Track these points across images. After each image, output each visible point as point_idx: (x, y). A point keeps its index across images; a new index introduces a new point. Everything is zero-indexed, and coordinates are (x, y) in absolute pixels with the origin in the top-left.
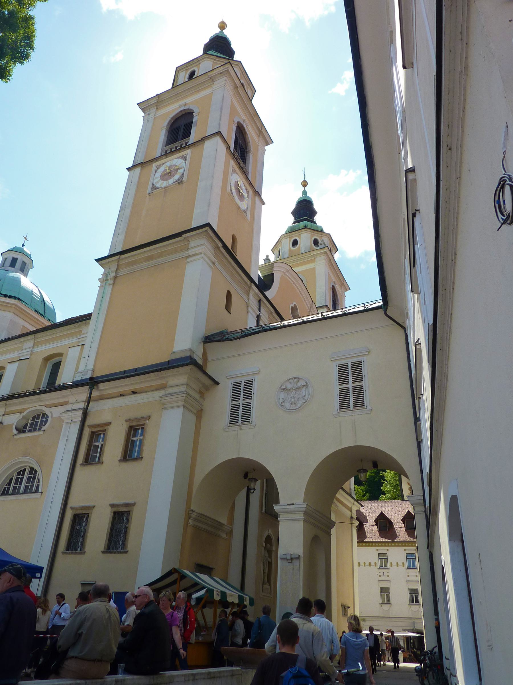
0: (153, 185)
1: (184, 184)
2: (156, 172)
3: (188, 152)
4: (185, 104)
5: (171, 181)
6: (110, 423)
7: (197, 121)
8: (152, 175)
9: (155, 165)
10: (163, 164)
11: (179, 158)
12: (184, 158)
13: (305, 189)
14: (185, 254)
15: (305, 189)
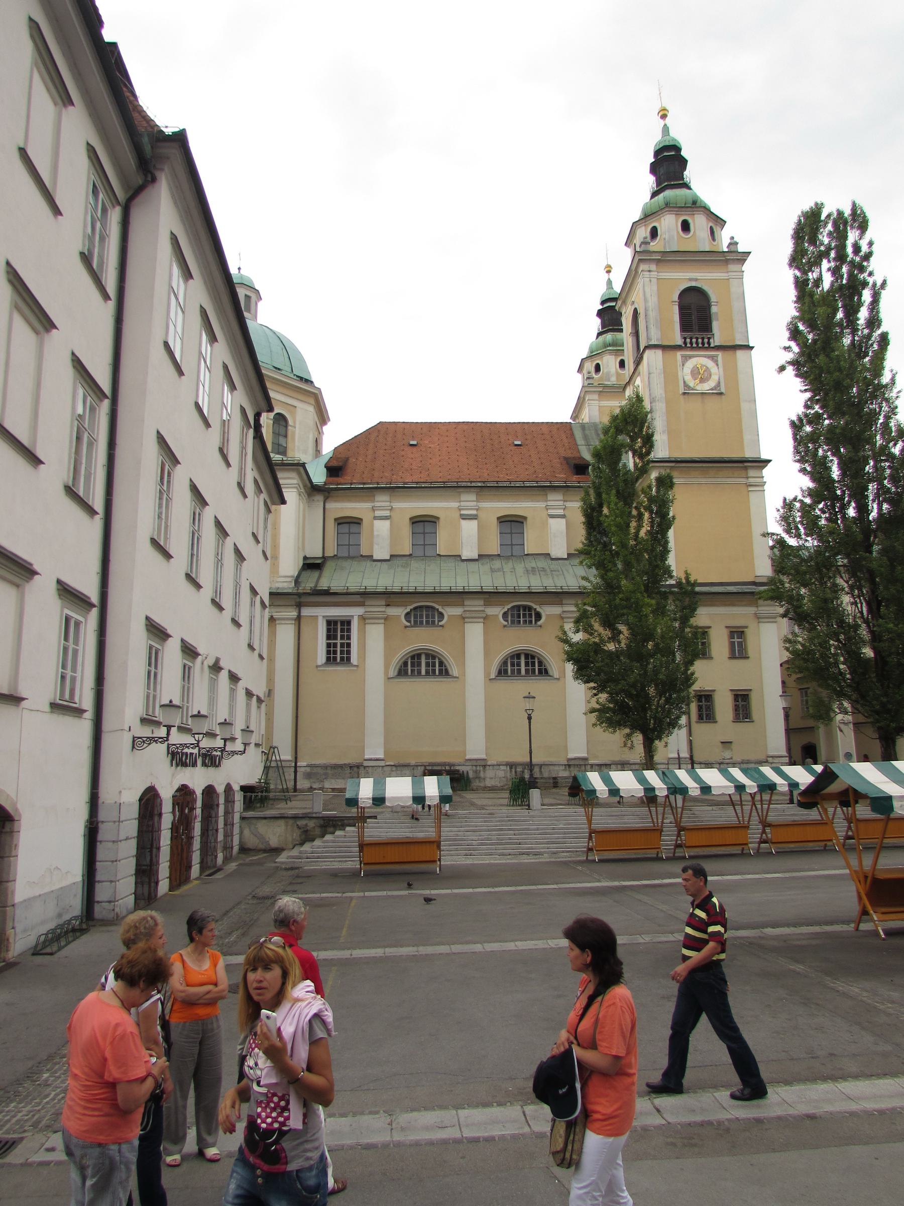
0: (684, 382)
1: (723, 397)
2: (683, 365)
3: (720, 354)
4: (696, 280)
5: (706, 387)
6: (710, 627)
7: (716, 313)
8: (679, 369)
9: (679, 354)
10: (691, 357)
11: (709, 357)
12: (713, 359)
13: (609, 279)
14: (743, 481)
15: (609, 279)
